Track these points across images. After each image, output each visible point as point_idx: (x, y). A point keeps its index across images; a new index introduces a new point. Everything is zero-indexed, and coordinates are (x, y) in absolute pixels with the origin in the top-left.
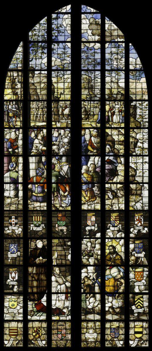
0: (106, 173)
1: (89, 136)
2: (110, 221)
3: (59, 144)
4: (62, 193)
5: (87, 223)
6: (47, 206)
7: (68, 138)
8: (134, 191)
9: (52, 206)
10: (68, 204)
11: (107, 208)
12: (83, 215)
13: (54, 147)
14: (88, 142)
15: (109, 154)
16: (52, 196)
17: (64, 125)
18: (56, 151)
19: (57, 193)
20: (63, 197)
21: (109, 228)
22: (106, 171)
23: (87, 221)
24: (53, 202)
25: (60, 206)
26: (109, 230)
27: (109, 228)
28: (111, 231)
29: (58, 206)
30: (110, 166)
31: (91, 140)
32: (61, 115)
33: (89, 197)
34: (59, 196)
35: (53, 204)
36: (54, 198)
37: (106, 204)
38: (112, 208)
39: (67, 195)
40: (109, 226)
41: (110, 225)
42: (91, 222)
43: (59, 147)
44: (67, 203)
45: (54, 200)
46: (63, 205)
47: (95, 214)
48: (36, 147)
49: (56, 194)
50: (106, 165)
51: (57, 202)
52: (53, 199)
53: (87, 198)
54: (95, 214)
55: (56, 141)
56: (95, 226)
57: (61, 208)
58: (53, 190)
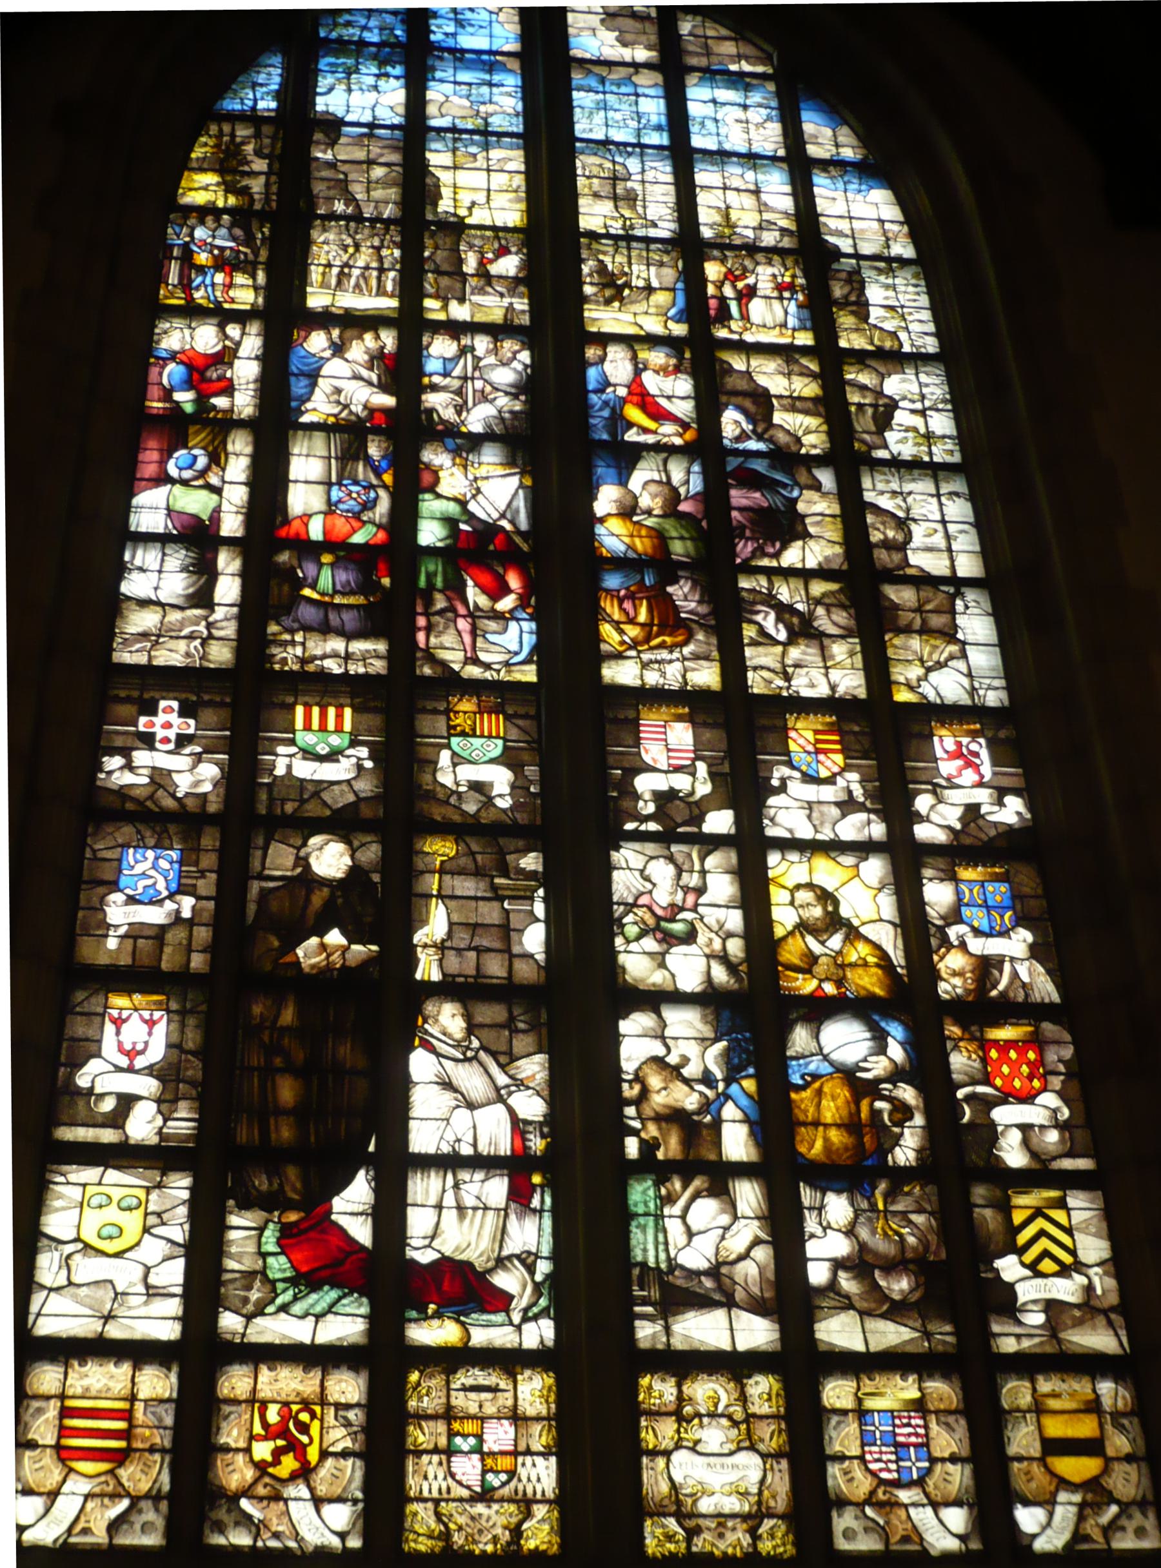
0: (734, 523)
2: (787, 753)
4: (483, 601)
5: (639, 754)
6: (390, 657)
8: (905, 617)
9: (419, 655)
10: (516, 654)
11: (757, 683)
12: (611, 715)
14: (622, 392)
15: (741, 446)
16: (419, 609)
19: (449, 599)
20: (489, 618)
21: (783, 788)
22: (735, 514)
23: (637, 744)
24: (421, 637)
25: (466, 658)
26: (783, 795)
27: (783, 788)
28: (799, 804)
29: (454, 658)
30: (757, 495)
31: (642, 385)
33: (642, 625)
34: (462, 610)
35: (422, 644)
36: (429, 621)
37: (748, 663)
38: (788, 688)
39: (511, 611)
40: (783, 781)
41: (785, 771)
42: (669, 750)
44: (514, 647)
45: (429, 629)
46: (483, 656)
47: (687, 710)
49: (440, 603)
50: (733, 492)
51: (449, 639)
52: (421, 621)
53: (633, 631)
54: (687, 710)
56: (693, 774)
57: (474, 672)
58: (422, 582)
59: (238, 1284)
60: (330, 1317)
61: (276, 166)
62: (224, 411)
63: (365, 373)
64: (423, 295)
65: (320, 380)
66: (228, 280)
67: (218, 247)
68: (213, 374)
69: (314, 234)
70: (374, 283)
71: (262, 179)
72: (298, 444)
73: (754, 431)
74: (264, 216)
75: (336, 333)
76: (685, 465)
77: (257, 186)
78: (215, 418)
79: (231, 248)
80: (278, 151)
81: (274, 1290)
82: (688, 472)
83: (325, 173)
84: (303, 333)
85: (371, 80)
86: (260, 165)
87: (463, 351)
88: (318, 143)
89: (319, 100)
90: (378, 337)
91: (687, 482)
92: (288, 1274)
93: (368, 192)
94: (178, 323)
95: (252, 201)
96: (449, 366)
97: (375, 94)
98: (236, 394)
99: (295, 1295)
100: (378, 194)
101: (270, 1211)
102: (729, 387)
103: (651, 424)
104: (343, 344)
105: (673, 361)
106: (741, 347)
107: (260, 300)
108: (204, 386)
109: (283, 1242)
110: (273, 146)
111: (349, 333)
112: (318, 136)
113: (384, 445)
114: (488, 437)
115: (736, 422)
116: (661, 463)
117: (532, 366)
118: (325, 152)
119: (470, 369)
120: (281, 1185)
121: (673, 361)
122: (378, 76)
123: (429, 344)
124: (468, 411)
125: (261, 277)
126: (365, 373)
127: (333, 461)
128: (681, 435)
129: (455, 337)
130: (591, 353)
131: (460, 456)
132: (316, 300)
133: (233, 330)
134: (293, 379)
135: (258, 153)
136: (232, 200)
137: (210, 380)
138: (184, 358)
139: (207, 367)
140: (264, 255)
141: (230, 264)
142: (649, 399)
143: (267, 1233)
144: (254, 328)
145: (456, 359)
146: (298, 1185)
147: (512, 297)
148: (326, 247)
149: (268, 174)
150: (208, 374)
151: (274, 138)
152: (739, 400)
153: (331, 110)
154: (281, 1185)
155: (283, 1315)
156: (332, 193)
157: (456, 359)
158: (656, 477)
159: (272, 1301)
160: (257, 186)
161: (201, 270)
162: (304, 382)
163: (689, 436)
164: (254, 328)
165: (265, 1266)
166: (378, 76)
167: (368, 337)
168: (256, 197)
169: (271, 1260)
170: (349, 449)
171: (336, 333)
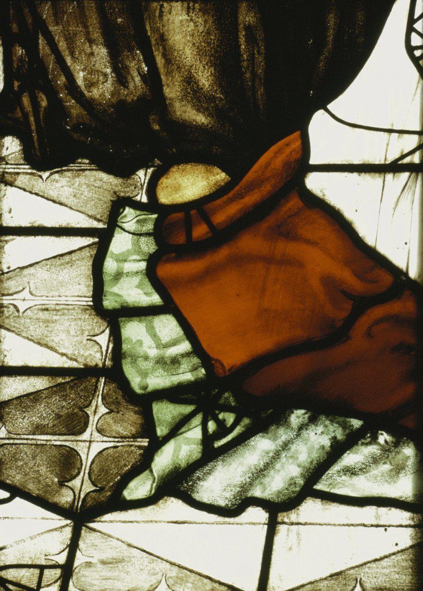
59: (43, 413)
60: (310, 508)
81: (147, 427)
92: (186, 375)
99: (207, 440)
101: (124, 171)
109: (166, 270)
120: (153, 79)
143: (120, 243)
146: (205, 79)
154: (153, 79)
155: (173, 507)
159: (144, 464)
165: (118, 353)
169: (133, 330)
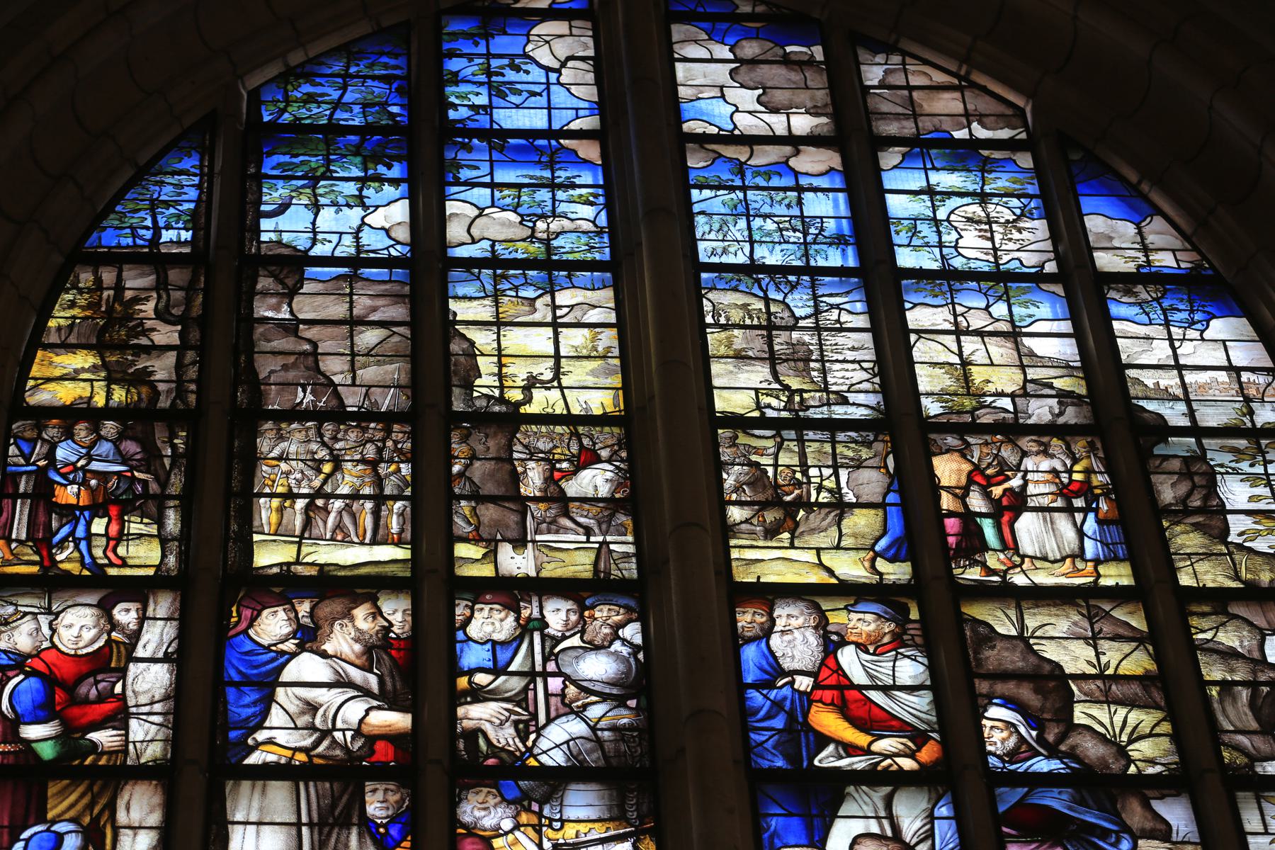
1: (813, 640)
3: (526, 689)
7: (616, 653)
13: (476, 714)
17: (579, 564)
18: (505, 737)
32: (535, 499)
43: (535, 716)
48: (303, 713)
55: (498, 670)
61: (195, 335)
62: (110, 753)
63: (356, 675)
64: (452, 539)
65: (280, 693)
66: (114, 529)
67: (96, 474)
68: (89, 690)
69: (264, 445)
70: (368, 522)
71: (171, 358)
72: (243, 802)
73: (1040, 740)
74: (173, 418)
75: (304, 608)
76: (924, 805)
77: (162, 368)
78: (94, 764)
79: (118, 473)
80: (196, 310)
82: (931, 818)
83: (278, 344)
84: (247, 613)
85: (351, 188)
86: (166, 335)
87: (526, 629)
88: (265, 294)
89: (265, 224)
90: (377, 613)
91: (930, 835)
93: (353, 370)
94: (28, 603)
95: (156, 394)
96: (503, 656)
97: (358, 212)
98: (133, 723)
100: (369, 374)
102: (991, 666)
103: (861, 739)
104: (318, 627)
105: (888, 627)
106: (1005, 593)
107: (172, 560)
108: (75, 711)
110: (188, 302)
111: (327, 609)
112: (264, 283)
113: (393, 798)
114: (575, 773)
115: (1009, 724)
116: (880, 805)
117: (646, 646)
118: (277, 308)
119: (538, 658)
121: (888, 627)
122: (363, 181)
123: (468, 621)
124: (539, 732)
125: (172, 521)
126: (356, 675)
127: (305, 830)
128: (912, 755)
129: (513, 607)
130: (747, 619)
131: (528, 810)
132: (268, 556)
133: (126, 614)
134: (231, 693)
135: (162, 315)
136: (119, 395)
137: (86, 701)
138: (40, 666)
139: (80, 679)
140: (176, 484)
141: (117, 501)
142: (851, 695)
144: (162, 605)
145: (513, 643)
147: (605, 534)
148: (284, 466)
149: (180, 349)
150: (83, 690)
151: (190, 289)
152: (1009, 688)
153: (286, 238)
156: (291, 375)
157: (513, 643)
158: (874, 828)
160: (162, 368)
161: (69, 512)
162: (251, 696)
163: (928, 753)
164: (162, 605)
166: (363, 181)
167: (361, 613)
168: (162, 387)
170: (333, 806)
171: (304, 608)
